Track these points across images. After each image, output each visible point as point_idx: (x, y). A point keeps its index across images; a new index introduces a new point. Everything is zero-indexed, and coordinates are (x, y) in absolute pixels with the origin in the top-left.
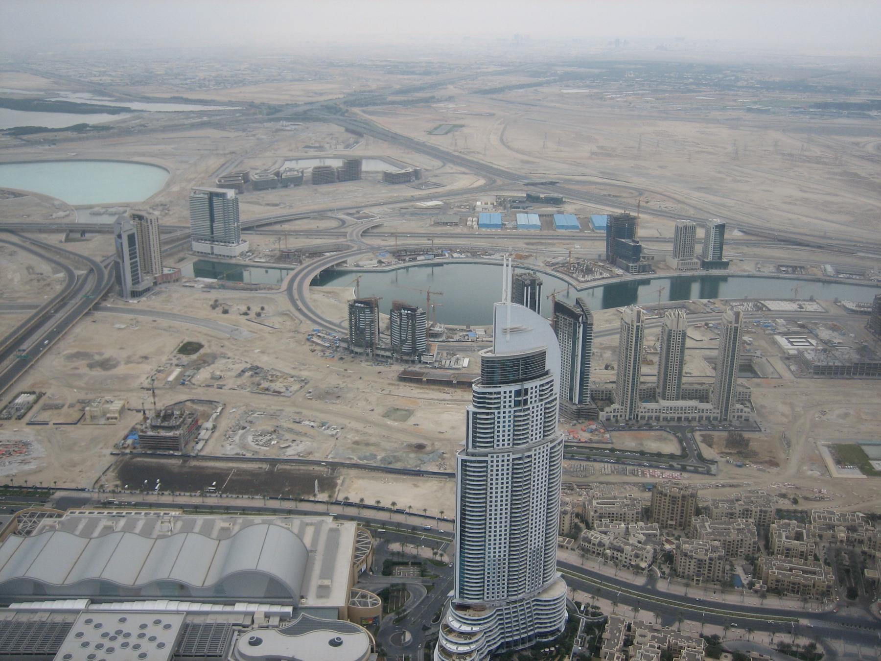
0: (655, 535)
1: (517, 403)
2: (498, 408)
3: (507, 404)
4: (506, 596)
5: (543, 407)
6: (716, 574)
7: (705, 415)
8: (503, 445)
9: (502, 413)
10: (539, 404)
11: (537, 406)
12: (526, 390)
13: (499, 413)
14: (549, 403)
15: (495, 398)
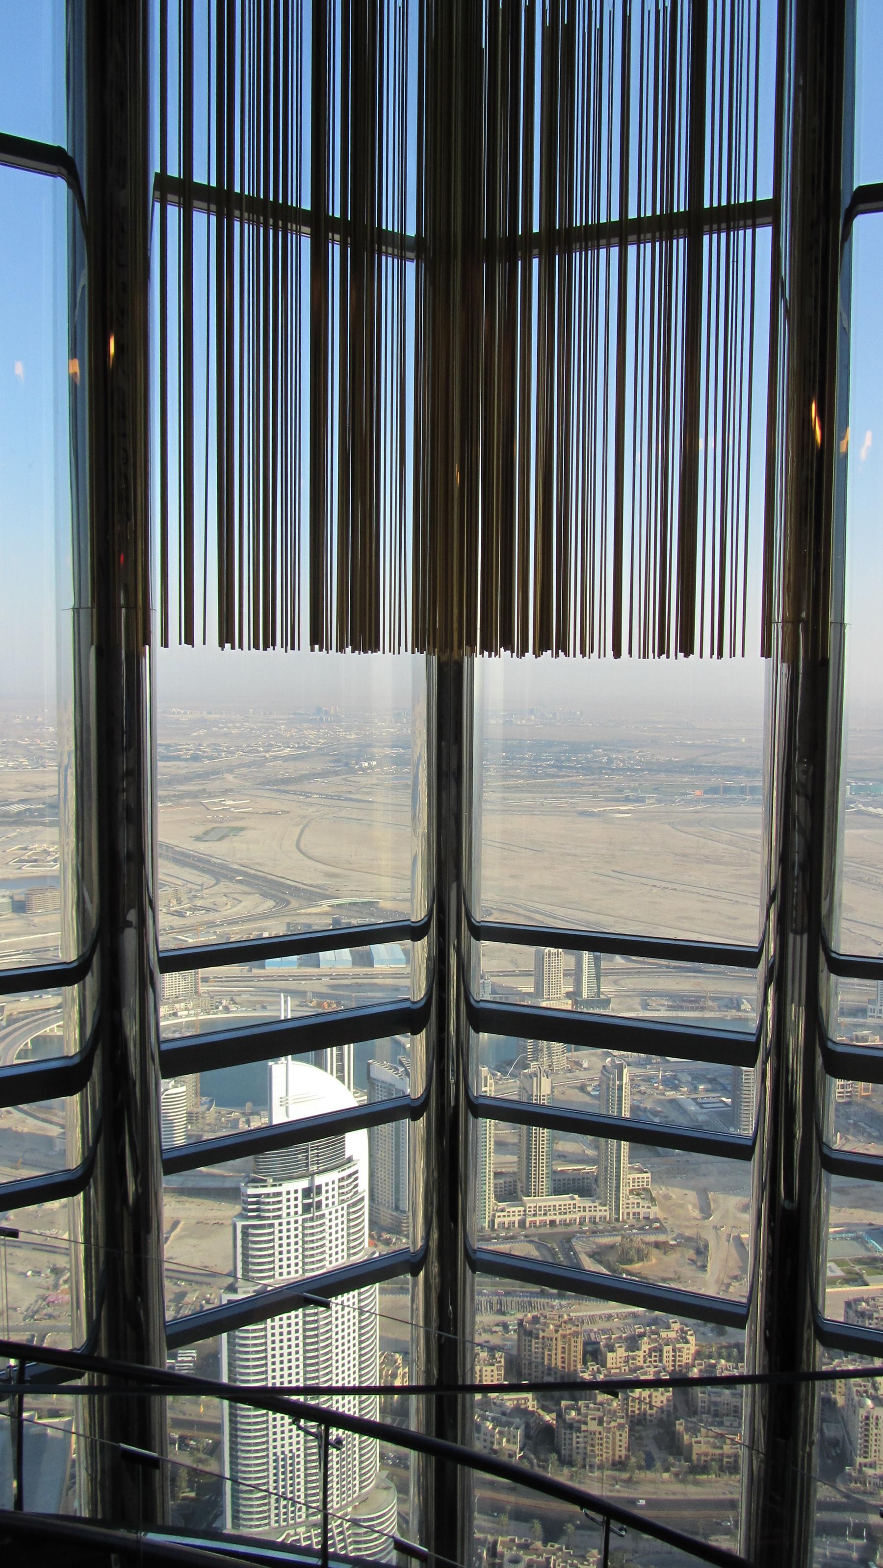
0: (526, 1399)
1: (307, 1208)
2: (279, 1217)
3: (292, 1210)
4: (304, 1516)
5: (345, 1212)
6: (617, 1453)
7: (587, 1214)
8: (289, 1273)
9: (284, 1224)
10: (339, 1208)
11: (337, 1211)
12: (319, 1187)
13: (280, 1224)
14: (354, 1204)
15: (274, 1203)
